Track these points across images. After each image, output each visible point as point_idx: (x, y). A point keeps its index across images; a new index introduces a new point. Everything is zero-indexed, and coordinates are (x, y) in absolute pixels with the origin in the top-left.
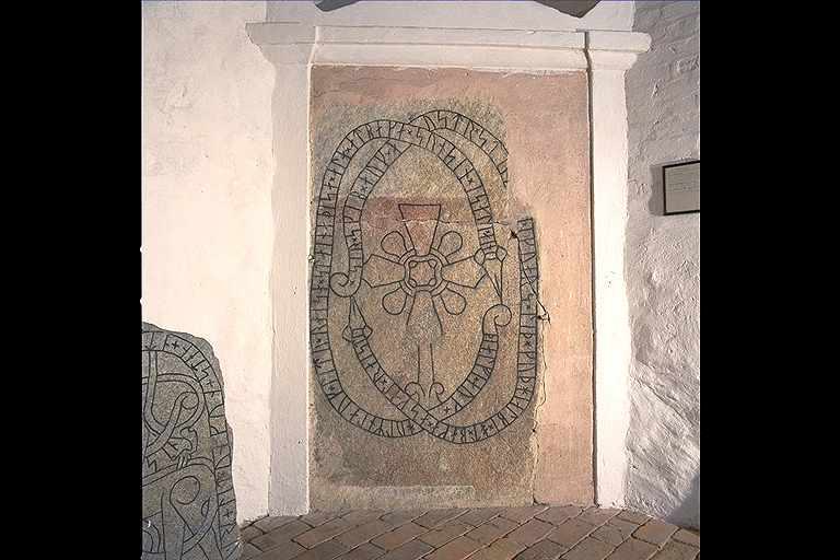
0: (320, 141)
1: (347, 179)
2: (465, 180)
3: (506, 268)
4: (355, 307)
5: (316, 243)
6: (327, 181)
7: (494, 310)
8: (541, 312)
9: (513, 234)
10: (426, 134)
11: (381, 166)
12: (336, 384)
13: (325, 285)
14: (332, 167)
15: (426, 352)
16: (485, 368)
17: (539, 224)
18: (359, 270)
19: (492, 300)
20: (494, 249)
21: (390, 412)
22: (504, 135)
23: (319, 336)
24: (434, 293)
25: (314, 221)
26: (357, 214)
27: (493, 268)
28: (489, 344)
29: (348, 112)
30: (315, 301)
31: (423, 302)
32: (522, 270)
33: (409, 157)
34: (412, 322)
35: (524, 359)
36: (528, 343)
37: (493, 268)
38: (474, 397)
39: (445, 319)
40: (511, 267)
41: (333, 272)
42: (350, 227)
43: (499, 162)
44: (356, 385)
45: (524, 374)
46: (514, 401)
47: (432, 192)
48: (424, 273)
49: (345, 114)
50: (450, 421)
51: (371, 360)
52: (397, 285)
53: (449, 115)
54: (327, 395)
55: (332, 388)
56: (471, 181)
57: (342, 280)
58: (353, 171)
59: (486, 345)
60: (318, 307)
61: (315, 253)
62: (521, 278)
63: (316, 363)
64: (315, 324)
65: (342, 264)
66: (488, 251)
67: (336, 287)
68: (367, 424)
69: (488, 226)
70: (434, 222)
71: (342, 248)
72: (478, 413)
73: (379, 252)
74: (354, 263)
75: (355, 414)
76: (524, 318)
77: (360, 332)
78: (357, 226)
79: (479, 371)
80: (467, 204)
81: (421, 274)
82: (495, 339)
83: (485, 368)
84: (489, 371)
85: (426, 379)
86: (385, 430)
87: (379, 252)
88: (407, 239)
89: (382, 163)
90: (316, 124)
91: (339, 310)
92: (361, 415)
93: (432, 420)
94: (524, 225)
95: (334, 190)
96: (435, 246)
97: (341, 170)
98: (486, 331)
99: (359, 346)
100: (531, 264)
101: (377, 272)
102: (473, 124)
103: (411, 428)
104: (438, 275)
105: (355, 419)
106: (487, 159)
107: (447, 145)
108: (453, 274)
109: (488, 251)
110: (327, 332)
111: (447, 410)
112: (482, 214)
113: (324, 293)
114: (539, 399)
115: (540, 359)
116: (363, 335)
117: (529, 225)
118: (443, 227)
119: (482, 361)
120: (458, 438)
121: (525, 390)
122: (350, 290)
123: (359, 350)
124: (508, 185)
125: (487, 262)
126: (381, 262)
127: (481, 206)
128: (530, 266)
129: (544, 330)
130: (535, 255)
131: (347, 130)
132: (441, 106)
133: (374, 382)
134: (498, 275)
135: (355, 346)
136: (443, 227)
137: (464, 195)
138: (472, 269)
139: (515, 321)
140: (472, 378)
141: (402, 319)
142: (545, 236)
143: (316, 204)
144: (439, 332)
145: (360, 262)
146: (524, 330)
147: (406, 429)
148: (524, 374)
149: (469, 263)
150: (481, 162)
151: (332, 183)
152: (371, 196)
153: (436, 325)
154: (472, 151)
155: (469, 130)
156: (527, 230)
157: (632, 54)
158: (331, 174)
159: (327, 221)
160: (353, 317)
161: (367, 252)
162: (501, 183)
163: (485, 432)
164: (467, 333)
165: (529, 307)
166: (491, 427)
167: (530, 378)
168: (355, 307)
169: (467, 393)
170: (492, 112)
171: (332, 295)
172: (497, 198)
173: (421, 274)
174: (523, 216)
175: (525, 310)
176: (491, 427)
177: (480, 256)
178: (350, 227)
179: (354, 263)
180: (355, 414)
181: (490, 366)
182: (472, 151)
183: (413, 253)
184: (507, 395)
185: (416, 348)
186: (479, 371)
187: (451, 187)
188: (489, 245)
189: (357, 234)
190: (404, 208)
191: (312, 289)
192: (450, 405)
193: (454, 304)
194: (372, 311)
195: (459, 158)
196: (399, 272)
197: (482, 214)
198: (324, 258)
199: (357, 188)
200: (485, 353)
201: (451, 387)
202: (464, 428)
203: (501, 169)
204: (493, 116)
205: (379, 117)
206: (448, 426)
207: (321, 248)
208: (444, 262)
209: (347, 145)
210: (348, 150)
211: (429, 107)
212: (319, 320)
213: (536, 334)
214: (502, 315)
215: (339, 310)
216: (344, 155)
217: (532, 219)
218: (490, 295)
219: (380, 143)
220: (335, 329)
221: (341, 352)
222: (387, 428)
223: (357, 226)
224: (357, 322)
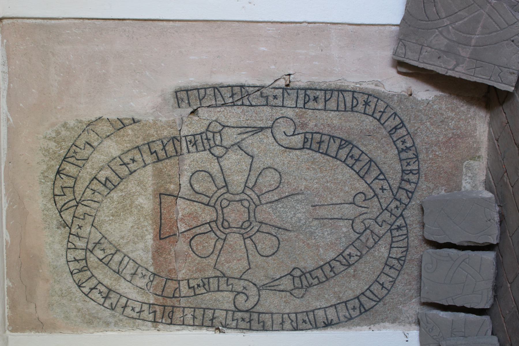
0: (91, 321)
1: (133, 294)
2: (133, 166)
3: (231, 122)
5: (202, 325)
6: (135, 315)
7: (278, 137)
8: (282, 83)
9: (192, 113)
10: (81, 209)
11: (117, 258)
12: (350, 306)
13: (246, 315)
14: (119, 309)
15: (322, 212)
16: (340, 147)
17: (182, 82)
18: (231, 281)
19: (266, 138)
20: (210, 135)
21: (382, 250)
22: (81, 122)
23: (300, 321)
24: (258, 202)
25: (178, 327)
26: (170, 283)
27: (231, 136)
28: (313, 142)
29: (60, 293)
30: (263, 326)
31: (265, 213)
32: (233, 104)
33: (106, 228)
34: (286, 226)
35: (332, 104)
36: (316, 99)
37: (231, 136)
38: (371, 160)
39: (286, 190)
40: (232, 116)
41: (233, 308)
42: (184, 290)
43: (111, 128)
44: (350, 286)
45: (349, 105)
46: (377, 115)
47: (146, 202)
48: (240, 215)
49: (62, 296)
50: (395, 186)
51: (327, 269)
52: (248, 241)
53: (59, 183)
54: (361, 313)
55: (354, 308)
56: (133, 160)
57: (241, 298)
58: (124, 287)
59: (315, 146)
60: (269, 323)
61: (212, 326)
62: (243, 105)
63: (328, 324)
64: (287, 325)
65: (224, 299)
66: (212, 142)
67: (249, 305)
68: (393, 273)
69: (184, 144)
70: (180, 201)
71: (207, 299)
72: (388, 158)
73: (211, 261)
74: (223, 286)
75: (382, 285)
76: (287, 103)
77: (297, 280)
78: (184, 284)
79: (343, 153)
80: (160, 165)
81: (235, 215)
82: (309, 136)
83: (340, 147)
84: (345, 143)
85: (349, 211)
86: (399, 256)
87: (211, 261)
88: (198, 231)
89: (114, 257)
90: (75, 329)
91: (272, 302)
92: (383, 279)
93: (393, 206)
94: (182, 100)
95: (145, 307)
96: (206, 200)
97: (123, 301)
98: (300, 145)
99: (311, 280)
100: (227, 93)
101: (234, 266)
102: (67, 160)
103: (399, 228)
104: (238, 198)
105: (388, 285)
106: (107, 143)
107: (93, 187)
108: (237, 181)
109: (212, 142)
110: (296, 313)
111: (382, 189)
112: (170, 148)
113: (255, 316)
114: (377, 88)
115: (333, 86)
116: (300, 277)
117: (183, 96)
118: (185, 190)
119: (333, 151)
120: (413, 178)
121: (366, 103)
122: (253, 291)
123: (316, 281)
124: (136, 117)
125: (225, 143)
126: (222, 259)
127: (165, 149)
128: (229, 95)
129: (301, 80)
130: (217, 88)
131: (79, 294)
132: (49, 191)
133: (349, 265)
134: (239, 130)
135: (311, 285)
136: (185, 190)
137: (149, 168)
138: (233, 161)
139: (290, 113)
140: (350, 161)
141: (283, 236)
142: (194, 78)
143: (160, 326)
144: (300, 197)
145: (223, 281)
146: (301, 103)
147: (400, 232)
148: (349, 105)
149: (225, 163)
150: (112, 148)
151: (137, 310)
152: (152, 269)
153: (292, 201)
154: (99, 158)
155: (75, 162)
156: (186, 97)
157: (170, 307)
158: (128, 310)
159: (178, 314)
160: (281, 287)
161: (210, 273)
162: (135, 126)
163: (408, 149)
164: (307, 171)
165: (275, 97)
166: (404, 142)
167: (353, 97)
169: (364, 166)
170: (54, 135)
171: (258, 308)
172: (152, 131)
173: (235, 215)
174: (173, 101)
175: (279, 102)
176: (404, 142)
177: (218, 151)
178: (184, 290)
179: (223, 286)
180: (382, 285)
181: (338, 141)
182: (99, 158)
183: (213, 225)
184: (369, 123)
185: (316, 222)
186: (343, 153)
187: (140, 183)
188: (204, 141)
189: (193, 283)
190: (164, 234)
191: (250, 329)
192: (376, 185)
193: (269, 179)
194: (275, 268)
195: (107, 173)
196: (235, 239)
197: (170, 148)
198: (218, 317)
199: (142, 283)
200: (324, 146)
201: (361, 186)
202: (403, 171)
203: (121, 125)
204: (58, 133)
205: (63, 260)
206: (400, 188)
207: (209, 321)
208: (223, 191)
209: (95, 294)
210: (100, 293)
211: (51, 205)
212: (283, 323)
213: (306, 89)
214: (283, 127)
215: (272, 302)
216: (106, 298)
217: (176, 92)
218: (261, 141)
219: (92, 259)
220: (295, 304)
221: (318, 299)
222: (396, 253)
223: (184, 284)
224: (286, 283)
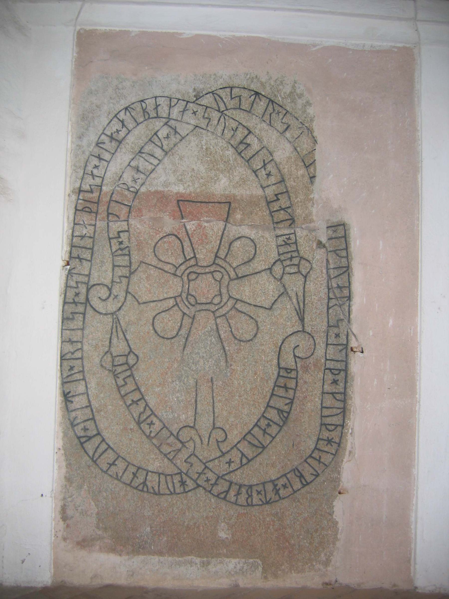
1: (114, 168)
3: (311, 286)
4: (117, 327)
5: (72, 246)
6: (90, 168)
7: (293, 338)
8: (353, 343)
10: (215, 115)
11: (158, 152)
13: (82, 298)
14: (97, 151)
15: (204, 390)
16: (280, 411)
18: (124, 281)
20: (296, 261)
24: (218, 314)
25: (72, 218)
26: (125, 210)
28: (286, 379)
30: (68, 319)
31: (205, 322)
33: (193, 141)
35: (329, 401)
36: (335, 382)
37: (294, 284)
38: (264, 448)
39: (231, 348)
41: (91, 283)
42: (115, 227)
43: (305, 152)
45: (328, 420)
47: (222, 186)
50: (234, 477)
51: (137, 396)
53: (245, 94)
56: (269, 175)
57: (104, 293)
59: (282, 381)
61: (71, 257)
62: (329, 299)
65: (102, 273)
66: (288, 262)
67: (95, 302)
69: (287, 232)
70: (221, 224)
71: (104, 252)
77: (122, 360)
78: (124, 226)
79: (273, 414)
81: (205, 288)
82: (293, 375)
83: (280, 411)
84: (285, 416)
85: (205, 423)
88: (187, 244)
91: (97, 330)
94: (335, 231)
95: (98, 181)
96: (222, 254)
97: (107, 156)
99: (122, 376)
104: (224, 291)
106: (288, 147)
108: (245, 290)
109: (288, 262)
111: (230, 463)
112: (282, 215)
113: (81, 309)
114: (347, 453)
115: (349, 402)
116: (127, 363)
117: (340, 232)
118: (234, 231)
122: (112, 306)
124: (317, 180)
125: (286, 277)
126: (153, 272)
127: (281, 208)
129: (356, 364)
132: (236, 82)
133: (139, 423)
134: (300, 294)
135: (116, 376)
136: (234, 231)
137: (260, 192)
139: (320, 351)
140: (263, 423)
143: (74, 197)
144: (223, 363)
145: (125, 271)
146: (330, 365)
149: (265, 276)
150: (283, 152)
151: (95, 172)
152: (143, 189)
154: (271, 137)
155: (268, 112)
158: (95, 161)
159: (86, 218)
160: (115, 341)
161: (135, 257)
162: (307, 179)
165: (337, 336)
167: (337, 426)
168: (117, 327)
171: (90, 312)
172: (301, 197)
174: (335, 220)
177: (278, 269)
178: (115, 227)
181: (286, 408)
183: (192, 262)
187: (244, 181)
189: (124, 236)
190: (184, 205)
191: (65, 303)
192: (235, 456)
193: (244, 328)
195: (256, 146)
196: (175, 286)
197: (282, 215)
199: (127, 178)
200: (281, 392)
201: (234, 436)
203: (308, 163)
204: (300, 96)
205: (158, 93)
207: (78, 253)
208: (232, 274)
209: (116, 125)
210: (118, 131)
212: (71, 342)
213: (346, 370)
214: (304, 343)
216: (111, 138)
217: (344, 225)
219: (158, 124)
220: (93, 358)
221: (98, 385)
224: (120, 347)
